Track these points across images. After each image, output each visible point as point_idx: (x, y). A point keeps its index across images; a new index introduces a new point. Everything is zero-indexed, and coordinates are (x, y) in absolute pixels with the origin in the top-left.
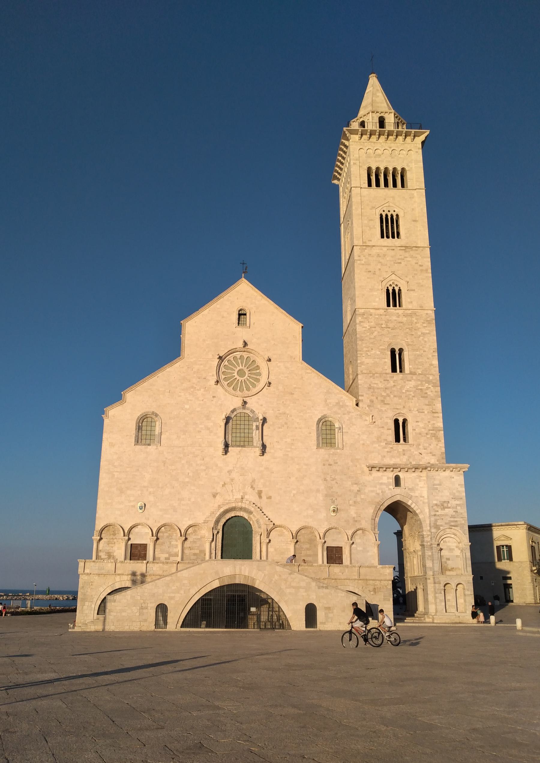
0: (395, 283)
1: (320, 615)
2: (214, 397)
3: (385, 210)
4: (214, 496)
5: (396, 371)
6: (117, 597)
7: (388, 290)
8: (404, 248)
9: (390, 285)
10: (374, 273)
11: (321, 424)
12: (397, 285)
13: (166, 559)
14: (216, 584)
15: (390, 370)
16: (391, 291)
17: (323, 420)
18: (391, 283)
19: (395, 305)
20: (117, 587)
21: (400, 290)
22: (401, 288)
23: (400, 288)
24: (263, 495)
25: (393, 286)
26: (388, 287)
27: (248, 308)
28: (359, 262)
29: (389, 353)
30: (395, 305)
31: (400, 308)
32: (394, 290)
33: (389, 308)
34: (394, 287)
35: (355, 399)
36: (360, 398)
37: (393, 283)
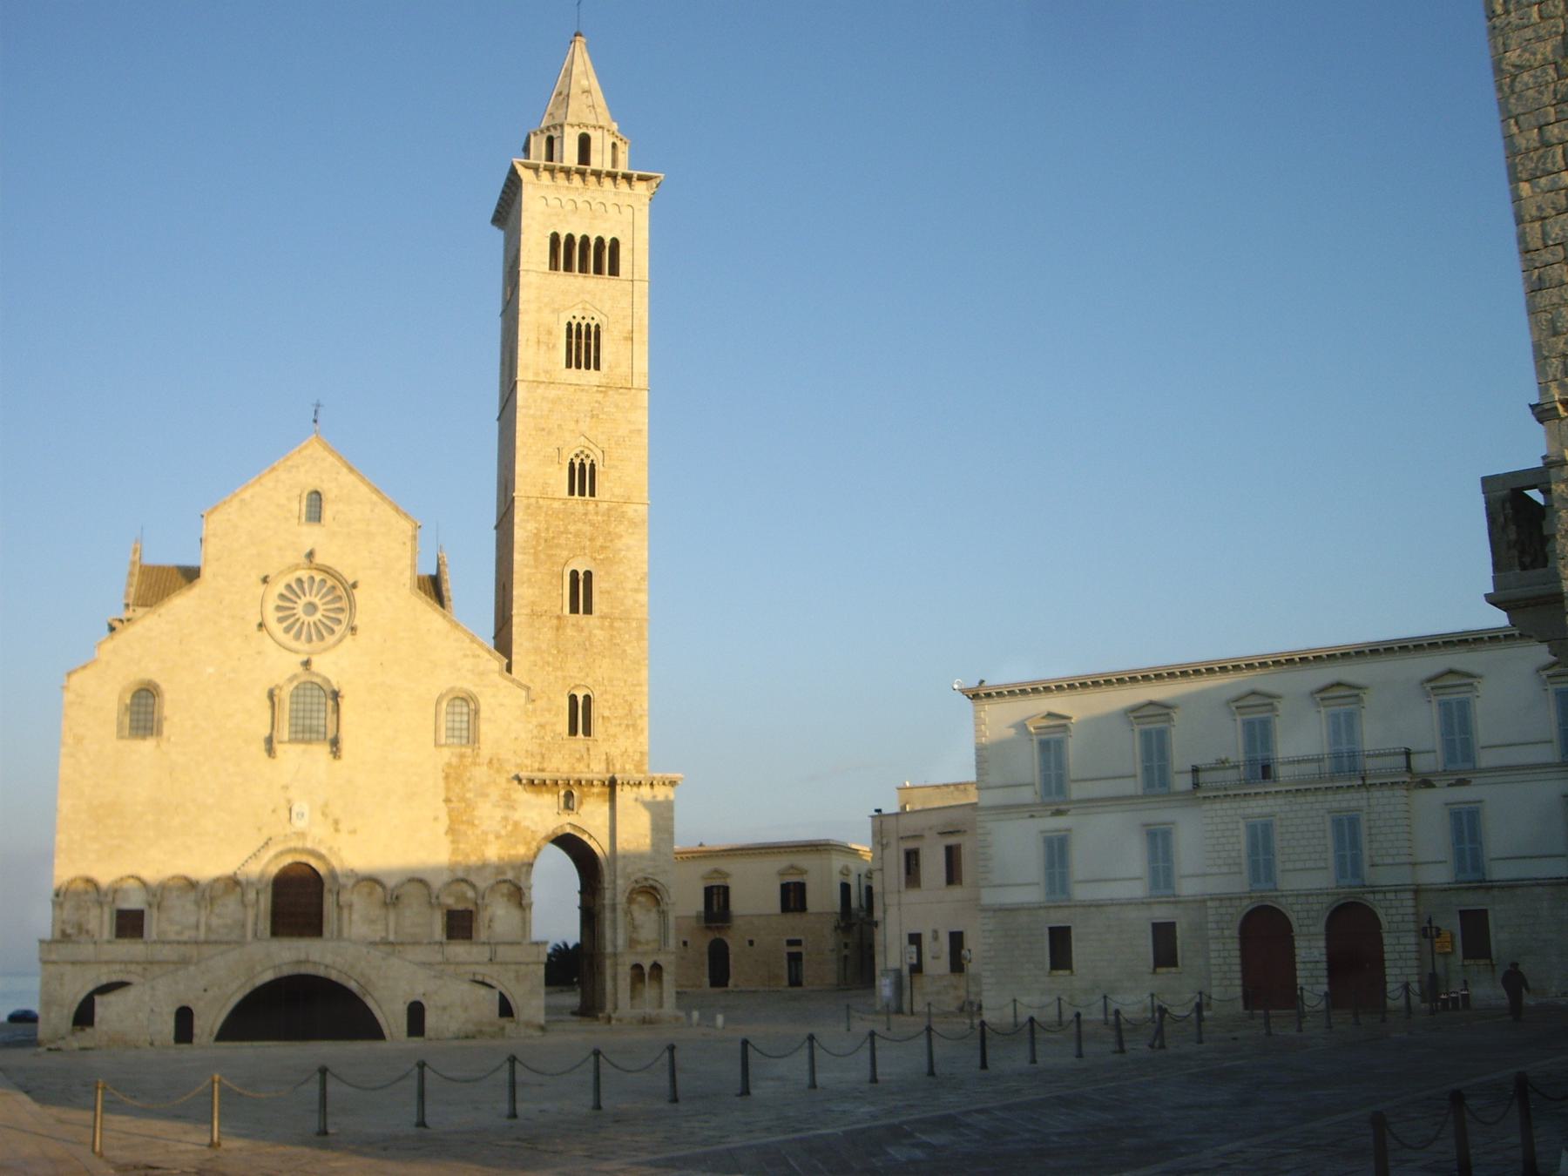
0: (587, 452)
1: (430, 1020)
2: (259, 653)
3: (576, 315)
4: (260, 829)
5: (578, 612)
6: (111, 998)
7: (572, 464)
8: (603, 389)
9: (577, 456)
10: (550, 433)
11: (444, 705)
12: (587, 456)
13: (178, 933)
14: (268, 976)
15: (567, 609)
16: (577, 466)
17: (451, 696)
18: (577, 451)
19: (582, 493)
20: (104, 980)
21: (592, 466)
22: (594, 462)
23: (592, 461)
24: (343, 826)
25: (583, 456)
26: (572, 460)
27: (330, 491)
28: (524, 411)
29: (567, 579)
30: (582, 493)
31: (592, 498)
32: (582, 465)
33: (572, 497)
34: (582, 460)
35: (507, 661)
36: (514, 658)
37: (582, 452)
